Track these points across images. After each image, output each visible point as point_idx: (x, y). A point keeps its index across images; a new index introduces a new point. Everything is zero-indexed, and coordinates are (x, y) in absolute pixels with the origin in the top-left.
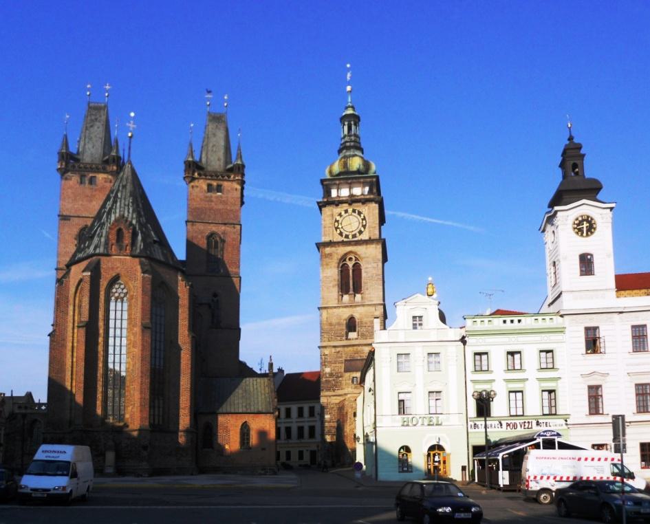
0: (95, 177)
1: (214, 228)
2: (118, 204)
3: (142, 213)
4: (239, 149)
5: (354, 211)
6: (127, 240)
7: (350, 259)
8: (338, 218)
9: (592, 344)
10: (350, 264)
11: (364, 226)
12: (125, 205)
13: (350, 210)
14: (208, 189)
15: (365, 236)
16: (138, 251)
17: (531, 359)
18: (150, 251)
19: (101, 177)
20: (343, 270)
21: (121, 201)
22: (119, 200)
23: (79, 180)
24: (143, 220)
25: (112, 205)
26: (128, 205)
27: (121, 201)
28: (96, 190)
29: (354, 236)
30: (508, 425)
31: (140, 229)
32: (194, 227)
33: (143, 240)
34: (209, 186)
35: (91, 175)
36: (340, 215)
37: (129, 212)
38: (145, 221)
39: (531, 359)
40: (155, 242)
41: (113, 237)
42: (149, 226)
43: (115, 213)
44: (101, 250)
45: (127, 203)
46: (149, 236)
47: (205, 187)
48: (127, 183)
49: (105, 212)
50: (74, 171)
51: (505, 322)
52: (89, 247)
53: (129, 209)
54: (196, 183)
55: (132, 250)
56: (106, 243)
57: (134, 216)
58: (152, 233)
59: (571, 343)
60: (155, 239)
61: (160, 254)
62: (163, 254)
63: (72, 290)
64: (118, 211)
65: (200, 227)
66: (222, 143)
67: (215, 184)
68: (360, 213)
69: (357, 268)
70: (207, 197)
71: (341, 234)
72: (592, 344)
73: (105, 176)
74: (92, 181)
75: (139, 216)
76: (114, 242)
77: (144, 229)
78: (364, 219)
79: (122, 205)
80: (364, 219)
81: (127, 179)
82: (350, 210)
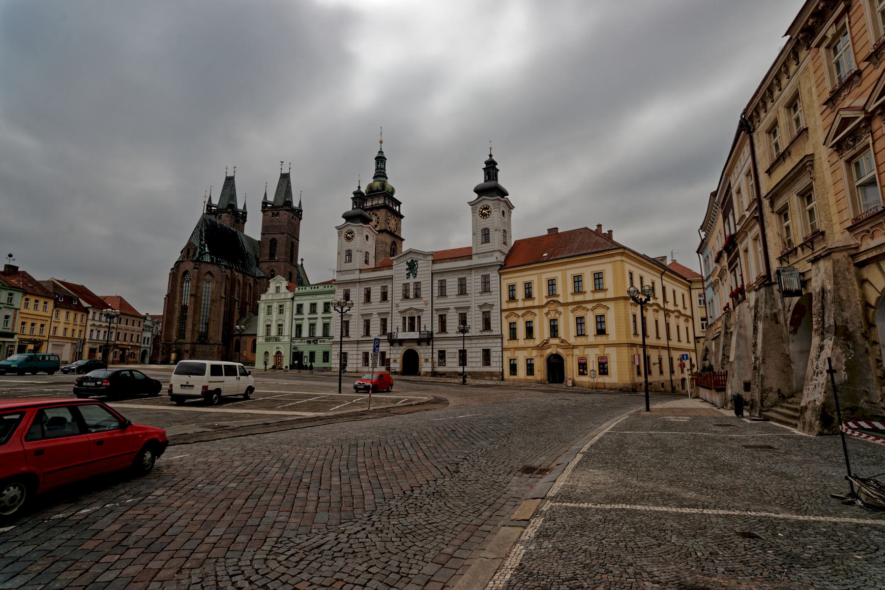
5: (373, 214)
6: (191, 254)
11: (378, 223)
13: (371, 214)
30: (307, 341)
33: (200, 253)
34: (273, 213)
40: (207, 253)
46: (205, 250)
47: (271, 215)
51: (325, 287)
54: (267, 213)
58: (206, 249)
62: (212, 259)
65: (268, 236)
67: (276, 212)
68: (376, 215)
73: (226, 214)
75: (202, 240)
78: (378, 218)
80: (378, 218)
82: (371, 214)
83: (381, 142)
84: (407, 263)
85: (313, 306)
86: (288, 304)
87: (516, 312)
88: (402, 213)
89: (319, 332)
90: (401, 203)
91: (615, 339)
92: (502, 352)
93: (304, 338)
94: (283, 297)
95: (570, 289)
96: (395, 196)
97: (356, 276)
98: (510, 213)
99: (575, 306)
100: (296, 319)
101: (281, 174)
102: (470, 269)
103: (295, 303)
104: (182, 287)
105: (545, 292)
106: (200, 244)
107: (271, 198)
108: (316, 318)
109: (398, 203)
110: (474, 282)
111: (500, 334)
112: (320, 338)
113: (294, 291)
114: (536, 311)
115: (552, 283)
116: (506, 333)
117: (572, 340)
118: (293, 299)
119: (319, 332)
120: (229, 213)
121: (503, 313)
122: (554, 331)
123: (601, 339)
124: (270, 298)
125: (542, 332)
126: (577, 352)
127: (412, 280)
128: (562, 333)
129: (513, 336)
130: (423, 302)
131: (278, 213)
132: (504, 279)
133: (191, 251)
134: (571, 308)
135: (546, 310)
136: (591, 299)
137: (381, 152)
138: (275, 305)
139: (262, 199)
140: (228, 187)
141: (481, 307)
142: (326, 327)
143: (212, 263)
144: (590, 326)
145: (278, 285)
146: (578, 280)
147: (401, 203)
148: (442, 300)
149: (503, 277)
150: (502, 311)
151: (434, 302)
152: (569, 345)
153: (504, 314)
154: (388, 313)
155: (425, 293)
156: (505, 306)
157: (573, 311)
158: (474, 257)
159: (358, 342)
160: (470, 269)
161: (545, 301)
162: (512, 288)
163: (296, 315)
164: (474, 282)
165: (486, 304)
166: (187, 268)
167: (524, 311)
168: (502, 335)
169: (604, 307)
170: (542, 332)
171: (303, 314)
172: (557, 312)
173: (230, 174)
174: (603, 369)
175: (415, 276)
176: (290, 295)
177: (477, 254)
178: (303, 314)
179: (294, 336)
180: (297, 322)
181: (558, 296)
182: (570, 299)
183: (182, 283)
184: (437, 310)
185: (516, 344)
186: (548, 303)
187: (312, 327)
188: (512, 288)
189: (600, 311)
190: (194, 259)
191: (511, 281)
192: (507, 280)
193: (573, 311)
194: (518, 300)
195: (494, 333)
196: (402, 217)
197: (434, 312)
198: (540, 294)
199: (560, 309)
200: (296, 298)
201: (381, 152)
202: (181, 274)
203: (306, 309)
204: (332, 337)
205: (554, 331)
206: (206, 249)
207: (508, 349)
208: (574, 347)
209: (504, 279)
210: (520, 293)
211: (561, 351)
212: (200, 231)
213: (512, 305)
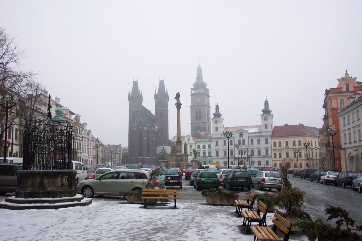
7: (198, 110)
8: (195, 99)
9: (217, 144)
10: (198, 111)
13: (198, 97)
15: (202, 104)
17: (207, 147)
20: (197, 113)
29: (199, 104)
36: (195, 98)
39: (207, 147)
59: (213, 144)
68: (200, 98)
69: (200, 112)
71: (196, 103)
72: (217, 144)
82: (198, 97)
83: (199, 61)
84: (239, 133)
85: (204, 147)
87: (276, 150)
88: (210, 94)
89: (207, 155)
90: (209, 90)
92: (272, 161)
93: (202, 157)
94: (191, 142)
96: (206, 87)
97: (220, 136)
98: (273, 118)
101: (160, 81)
102: (261, 136)
103: (197, 145)
105: (285, 145)
108: (200, 150)
109: (208, 90)
110: (263, 141)
112: (207, 157)
114: (282, 150)
115: (287, 143)
116: (273, 156)
117: (293, 158)
118: (196, 143)
119: (207, 155)
122: (287, 156)
125: (284, 156)
126: (294, 162)
127: (241, 139)
128: (290, 156)
129: (275, 157)
130: (245, 146)
134: (292, 150)
135: (285, 150)
137: (199, 66)
141: (265, 148)
142: (210, 153)
145: (189, 138)
146: (294, 142)
147: (209, 90)
148: (252, 145)
149: (272, 139)
150: (272, 149)
151: (249, 146)
152: (292, 159)
153: (273, 151)
154: (233, 149)
155: (246, 142)
156: (273, 148)
157: (293, 150)
158: (262, 133)
159: (222, 158)
160: (261, 136)
161: (285, 147)
162: (275, 143)
163: (197, 149)
164: (263, 141)
165: (267, 147)
167: (279, 150)
168: (272, 156)
170: (284, 156)
172: (288, 150)
174: (301, 166)
175: (242, 137)
181: (289, 146)
182: (292, 147)
184: (250, 148)
186: (286, 148)
187: (204, 153)
188: (275, 143)
191: (275, 141)
195: (269, 156)
196: (210, 96)
197: (250, 149)
198: (283, 145)
199: (289, 150)
200: (197, 143)
201: (199, 66)
203: (201, 147)
204: (212, 157)
205: (287, 156)
208: (293, 160)
210: (277, 145)
211: (289, 161)
213: (275, 148)
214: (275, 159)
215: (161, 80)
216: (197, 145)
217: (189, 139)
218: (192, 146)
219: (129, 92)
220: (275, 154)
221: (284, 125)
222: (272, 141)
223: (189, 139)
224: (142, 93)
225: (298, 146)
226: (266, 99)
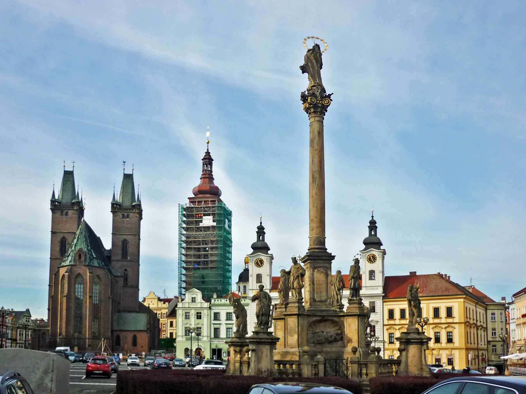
0: (68, 212)
1: (125, 237)
2: (79, 241)
3: (89, 245)
4: (138, 195)
6: (83, 259)
12: (82, 242)
14: (123, 217)
16: (87, 263)
18: (92, 263)
19: (70, 212)
21: (80, 240)
22: (79, 239)
23: (61, 214)
24: (89, 248)
25: (77, 242)
26: (83, 242)
27: (80, 240)
28: (68, 219)
31: (88, 253)
32: (116, 236)
33: (89, 258)
34: (123, 215)
35: (66, 211)
37: (83, 245)
38: (90, 248)
40: (95, 258)
41: (77, 257)
42: (92, 250)
43: (78, 245)
44: (72, 263)
45: (83, 241)
47: (121, 216)
48: (83, 231)
49: (73, 244)
50: (57, 210)
52: (67, 260)
53: (83, 243)
55: (85, 263)
56: (74, 260)
57: (86, 247)
58: (93, 253)
60: (94, 256)
61: (96, 263)
62: (98, 263)
63: (60, 278)
64: (79, 244)
66: (130, 191)
70: (122, 221)
73: (72, 211)
74: (67, 214)
75: (88, 246)
76: (77, 259)
77: (90, 253)
79: (81, 242)
81: (83, 229)
86: (205, 313)
87: (394, 327)
91: (458, 345)
92: (384, 351)
93: (223, 339)
94: (199, 306)
95: (431, 314)
99: (434, 326)
100: (214, 324)
101: (124, 174)
103: (213, 312)
104: (75, 288)
106: (87, 249)
107: (118, 198)
111: (382, 340)
113: (210, 301)
116: (387, 339)
118: (210, 308)
120: (76, 210)
121: (384, 327)
123: (450, 345)
124: (187, 305)
131: (128, 215)
132: (385, 305)
133: (82, 255)
134: (432, 326)
136: (445, 322)
138: (193, 313)
139: (111, 200)
140: (68, 182)
143: (99, 267)
144: (444, 338)
145: (193, 296)
150: (384, 325)
153: (385, 328)
156: (386, 322)
157: (433, 328)
163: (213, 320)
166: (79, 272)
168: (384, 340)
169: (452, 327)
171: (220, 320)
173: (69, 168)
176: (206, 305)
177: (366, 287)
178: (220, 320)
179: (213, 336)
180: (215, 326)
183: (75, 284)
185: (394, 346)
189: (449, 330)
190: (87, 264)
191: (391, 307)
192: (390, 306)
193: (433, 328)
194: (395, 319)
200: (213, 308)
202: (74, 277)
206: (93, 253)
207: (388, 349)
209: (385, 305)
212: (85, 237)
214: (436, 344)
215: (127, 172)
216: (213, 312)
217: (195, 298)
218: (200, 313)
219: (54, 192)
220: (391, 336)
221: (409, 274)
222: (384, 306)
223: (195, 298)
224: (82, 199)
225: (445, 318)
226: (373, 217)
